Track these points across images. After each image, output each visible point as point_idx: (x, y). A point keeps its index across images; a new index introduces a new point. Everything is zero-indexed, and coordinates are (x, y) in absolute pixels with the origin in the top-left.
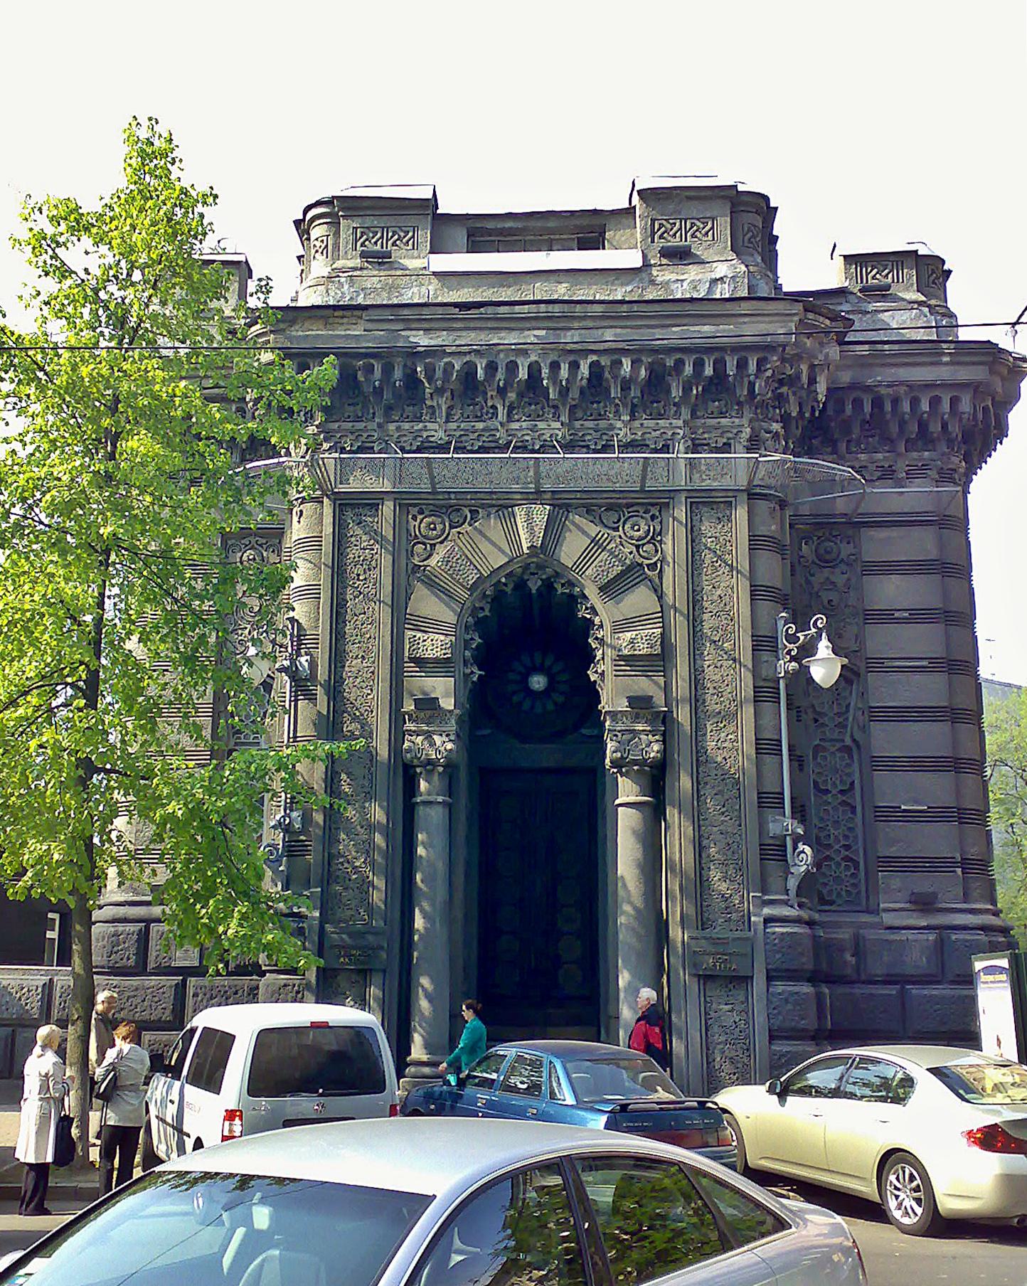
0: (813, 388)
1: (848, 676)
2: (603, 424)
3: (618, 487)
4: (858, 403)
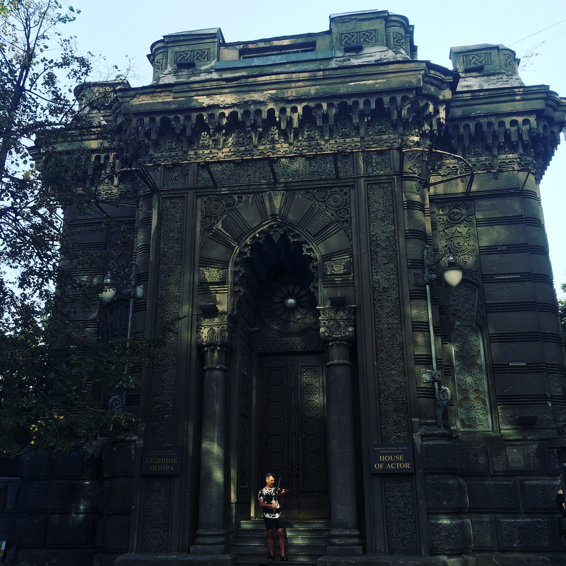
2: (314, 143)
4: (467, 127)
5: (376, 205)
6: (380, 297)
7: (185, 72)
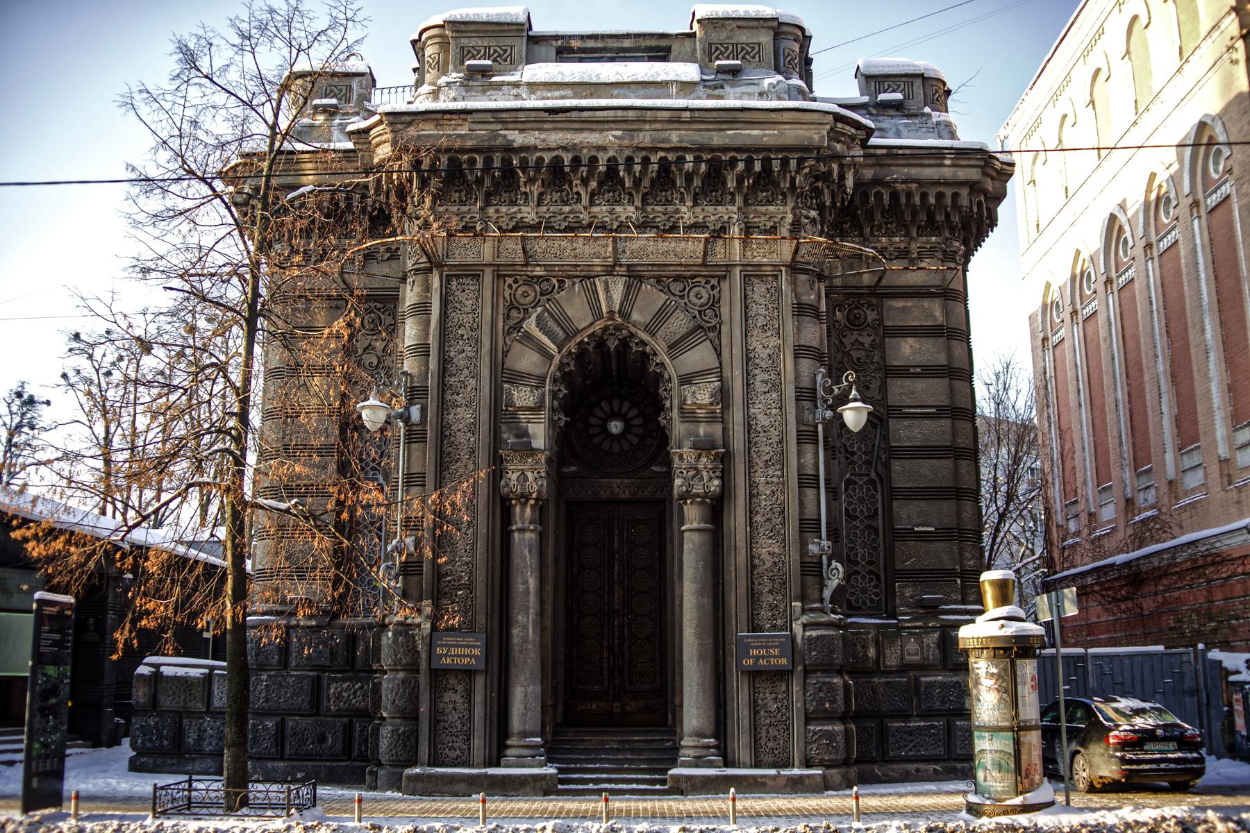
1: (876, 421)
2: (671, 208)
4: (879, 196)
7: (478, 82)
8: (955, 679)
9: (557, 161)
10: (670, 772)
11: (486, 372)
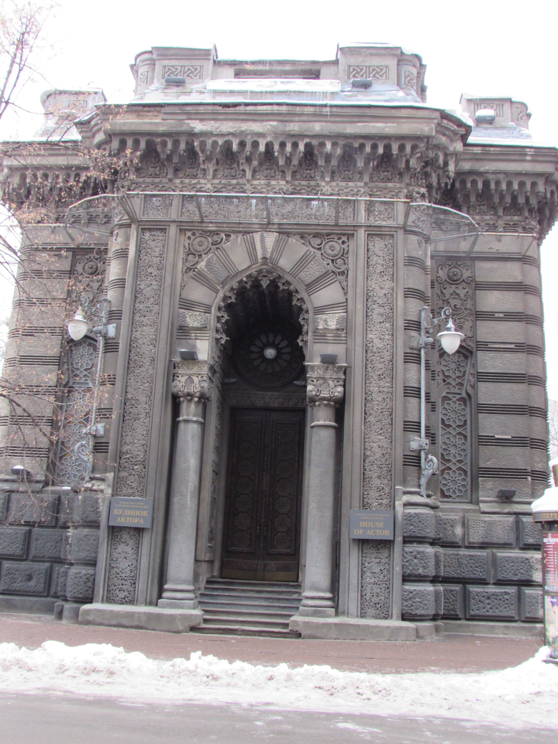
0: (446, 169)
1: (465, 352)
2: (313, 183)
3: (321, 222)
4: (474, 182)
5: (375, 258)
6: (373, 358)
7: (175, 90)
8: (524, 555)
9: (228, 144)
10: (292, 618)
11: (166, 301)
